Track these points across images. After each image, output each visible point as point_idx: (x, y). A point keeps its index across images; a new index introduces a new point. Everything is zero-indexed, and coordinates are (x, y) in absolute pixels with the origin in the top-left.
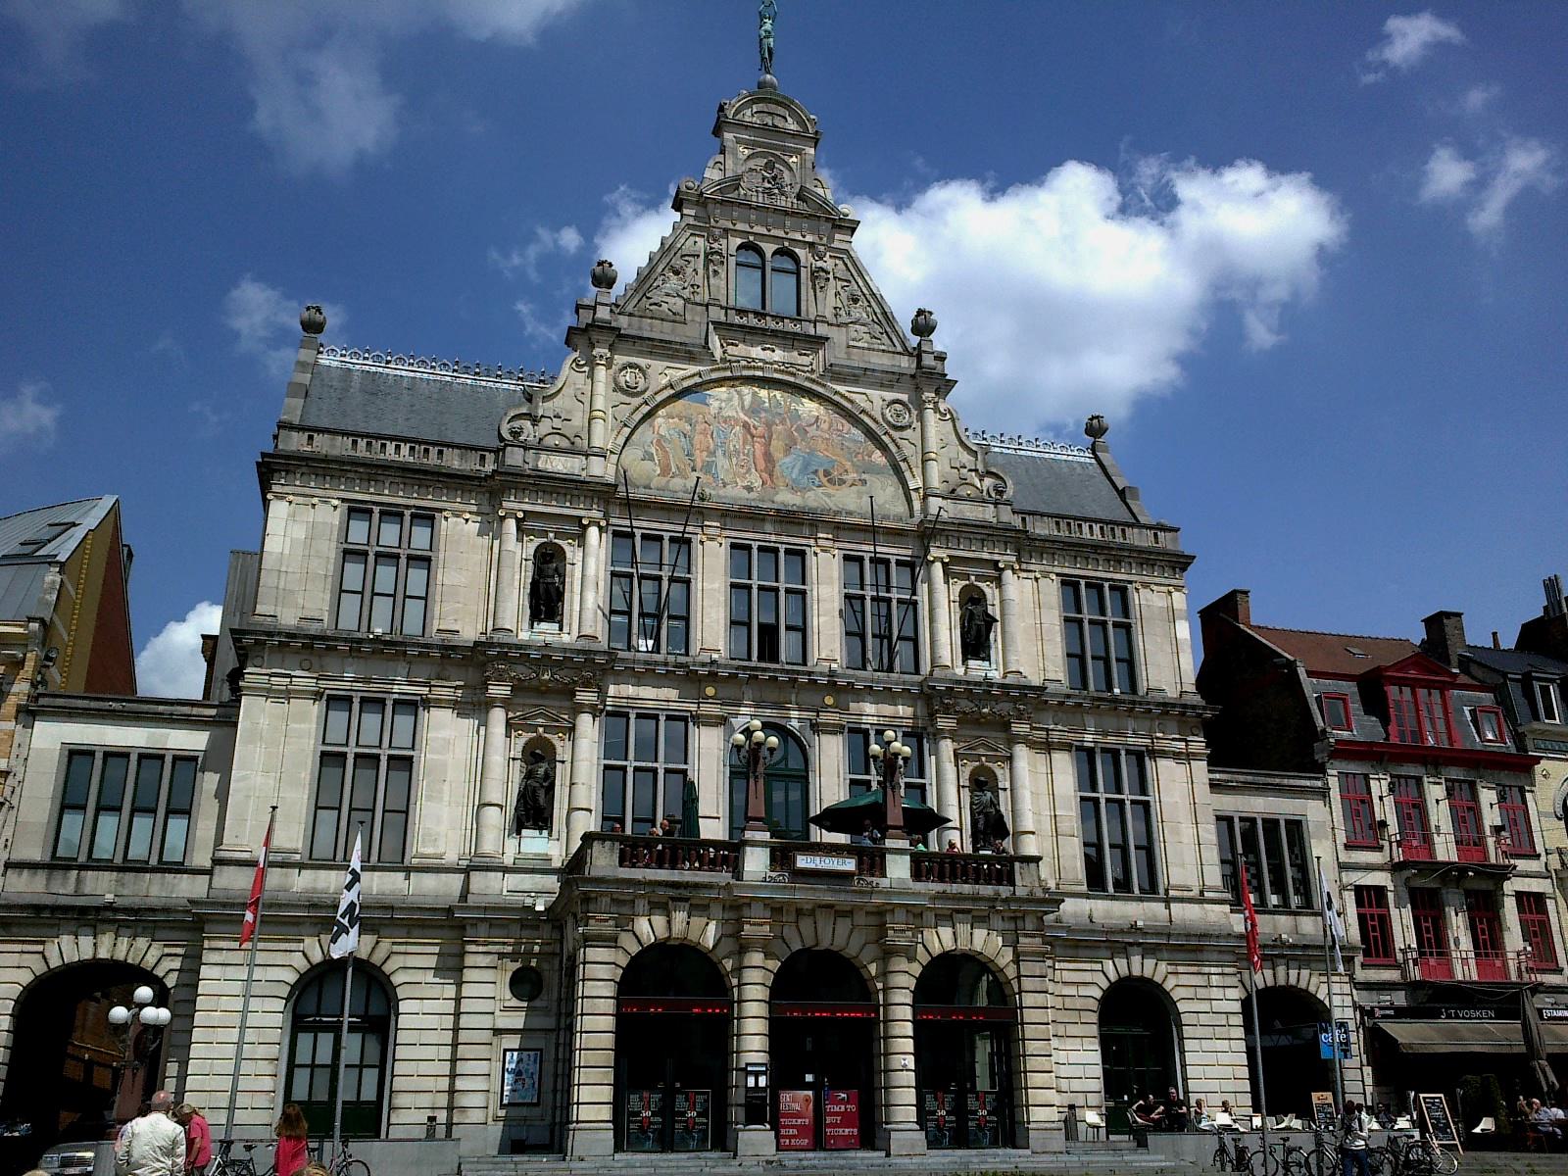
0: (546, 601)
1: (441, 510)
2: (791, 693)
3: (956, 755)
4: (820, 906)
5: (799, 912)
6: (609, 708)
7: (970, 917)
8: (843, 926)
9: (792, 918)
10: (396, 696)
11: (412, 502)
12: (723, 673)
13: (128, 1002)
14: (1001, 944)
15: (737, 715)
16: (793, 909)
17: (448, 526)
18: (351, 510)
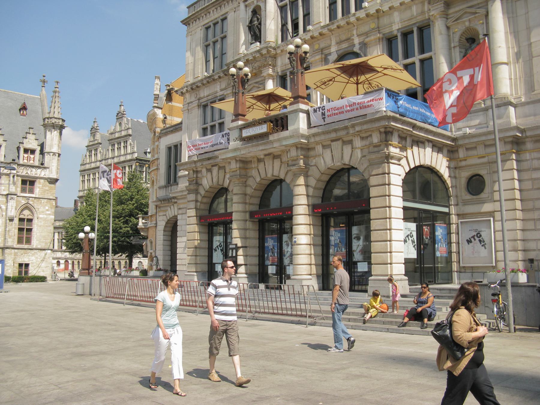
0: (256, 32)
1: (227, 13)
2: (353, 30)
3: (448, 28)
4: (265, 155)
5: (259, 160)
6: (280, 74)
7: (341, 141)
8: (277, 163)
9: (256, 165)
10: (219, 98)
11: (219, 15)
12: (316, 34)
13: (83, 231)
14: (359, 156)
15: (330, 54)
16: (256, 160)
17: (230, 17)
18: (207, 28)
